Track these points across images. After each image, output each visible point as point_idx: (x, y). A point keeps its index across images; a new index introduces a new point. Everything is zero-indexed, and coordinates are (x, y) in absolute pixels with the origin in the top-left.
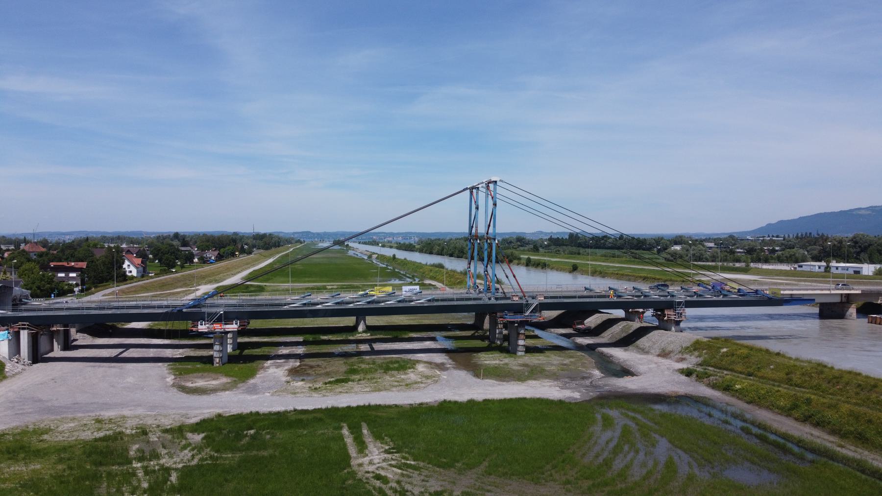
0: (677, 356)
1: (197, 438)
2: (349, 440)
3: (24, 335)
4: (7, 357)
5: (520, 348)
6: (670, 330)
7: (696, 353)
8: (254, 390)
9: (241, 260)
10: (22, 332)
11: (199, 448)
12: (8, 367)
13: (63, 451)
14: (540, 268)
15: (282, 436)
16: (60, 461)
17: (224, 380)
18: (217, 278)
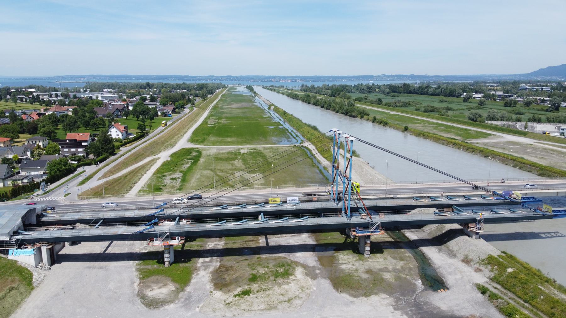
0: (475, 266)
3: (44, 249)
4: (34, 266)
6: (471, 237)
7: (489, 267)
9: (187, 117)
10: (42, 248)
14: (382, 126)
17: (171, 287)
18: (172, 141)
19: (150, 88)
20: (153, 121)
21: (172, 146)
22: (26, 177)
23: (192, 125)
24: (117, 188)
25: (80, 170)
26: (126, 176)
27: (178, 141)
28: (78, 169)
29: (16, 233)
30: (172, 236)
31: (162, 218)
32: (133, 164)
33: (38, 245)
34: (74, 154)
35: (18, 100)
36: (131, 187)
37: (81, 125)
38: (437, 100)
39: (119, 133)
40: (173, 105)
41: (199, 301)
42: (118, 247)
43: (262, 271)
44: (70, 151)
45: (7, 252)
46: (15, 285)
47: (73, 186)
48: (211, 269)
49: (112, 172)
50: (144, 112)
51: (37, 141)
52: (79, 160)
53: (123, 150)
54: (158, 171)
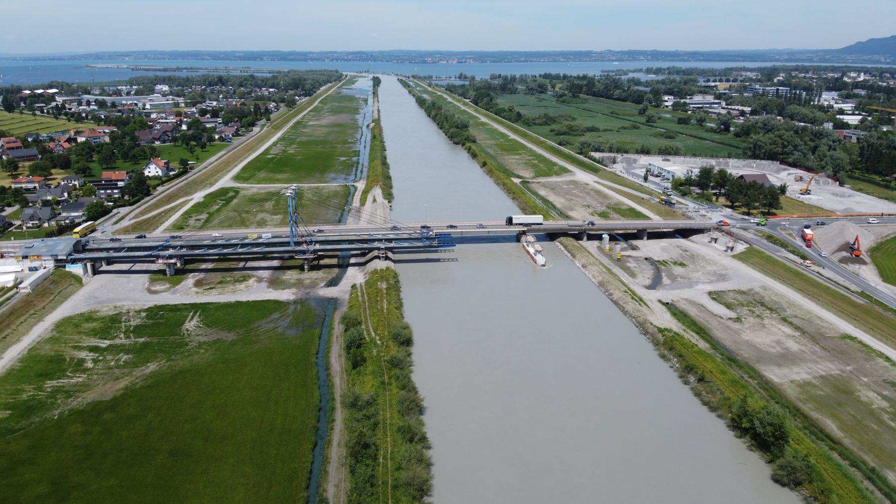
1: (144, 314)
2: (190, 317)
3: (89, 265)
8: (174, 293)
11: (143, 319)
12: (84, 280)
13: (103, 318)
15: (170, 314)
16: (102, 322)
17: (168, 286)
19: (223, 85)
20: (204, 150)
21: (211, 185)
22: (67, 218)
23: (249, 155)
24: (145, 227)
25: (115, 211)
26: (154, 217)
27: (221, 178)
28: (113, 211)
29: (70, 255)
30: (171, 257)
31: (166, 248)
32: (164, 206)
33: (85, 262)
34: (109, 195)
35: (36, 110)
36: (158, 227)
37: (120, 156)
38: (607, 111)
39: (158, 170)
40: (239, 124)
41: (181, 292)
42: (138, 267)
43: (229, 279)
44: (106, 193)
45: (64, 267)
46: (73, 283)
47: (109, 226)
48: (196, 279)
49: (142, 213)
50: (195, 137)
51: (73, 180)
52: (115, 201)
53: (160, 189)
54: (186, 213)
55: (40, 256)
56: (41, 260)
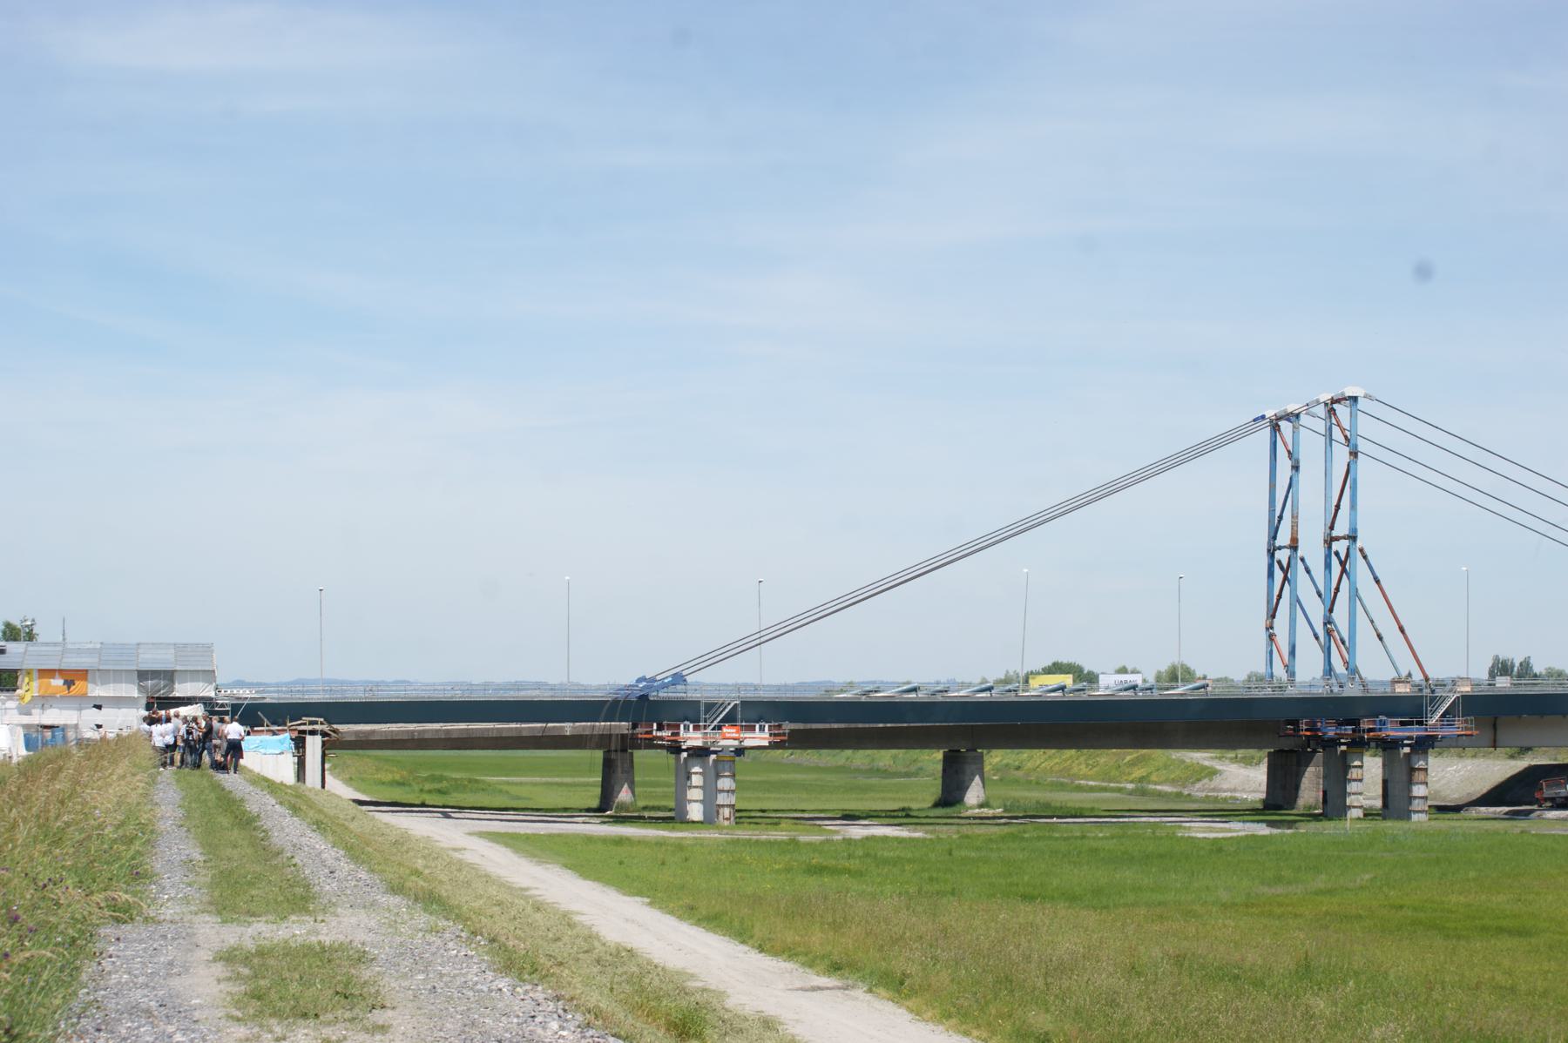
5: (1417, 805)
10: (309, 739)
55: (83, 674)
56: (83, 701)
